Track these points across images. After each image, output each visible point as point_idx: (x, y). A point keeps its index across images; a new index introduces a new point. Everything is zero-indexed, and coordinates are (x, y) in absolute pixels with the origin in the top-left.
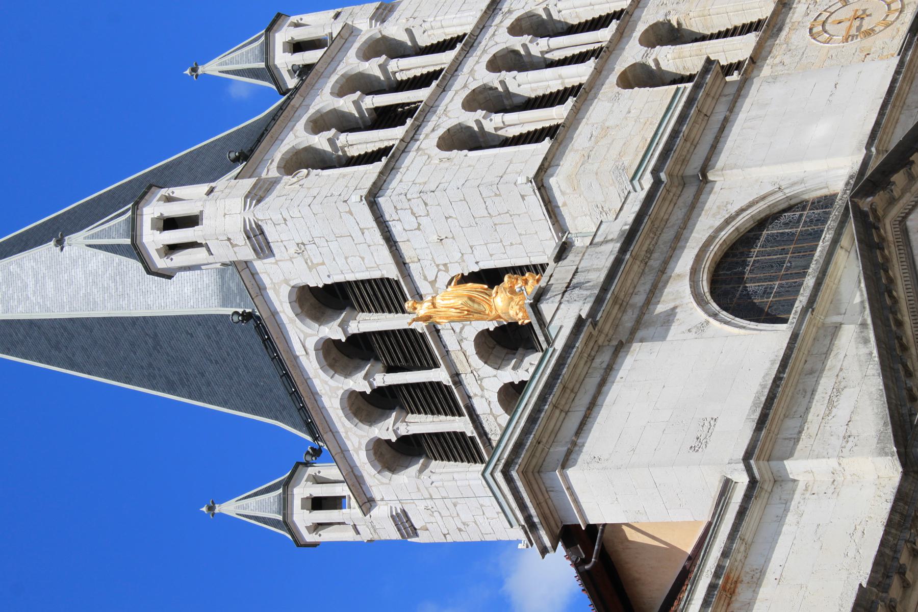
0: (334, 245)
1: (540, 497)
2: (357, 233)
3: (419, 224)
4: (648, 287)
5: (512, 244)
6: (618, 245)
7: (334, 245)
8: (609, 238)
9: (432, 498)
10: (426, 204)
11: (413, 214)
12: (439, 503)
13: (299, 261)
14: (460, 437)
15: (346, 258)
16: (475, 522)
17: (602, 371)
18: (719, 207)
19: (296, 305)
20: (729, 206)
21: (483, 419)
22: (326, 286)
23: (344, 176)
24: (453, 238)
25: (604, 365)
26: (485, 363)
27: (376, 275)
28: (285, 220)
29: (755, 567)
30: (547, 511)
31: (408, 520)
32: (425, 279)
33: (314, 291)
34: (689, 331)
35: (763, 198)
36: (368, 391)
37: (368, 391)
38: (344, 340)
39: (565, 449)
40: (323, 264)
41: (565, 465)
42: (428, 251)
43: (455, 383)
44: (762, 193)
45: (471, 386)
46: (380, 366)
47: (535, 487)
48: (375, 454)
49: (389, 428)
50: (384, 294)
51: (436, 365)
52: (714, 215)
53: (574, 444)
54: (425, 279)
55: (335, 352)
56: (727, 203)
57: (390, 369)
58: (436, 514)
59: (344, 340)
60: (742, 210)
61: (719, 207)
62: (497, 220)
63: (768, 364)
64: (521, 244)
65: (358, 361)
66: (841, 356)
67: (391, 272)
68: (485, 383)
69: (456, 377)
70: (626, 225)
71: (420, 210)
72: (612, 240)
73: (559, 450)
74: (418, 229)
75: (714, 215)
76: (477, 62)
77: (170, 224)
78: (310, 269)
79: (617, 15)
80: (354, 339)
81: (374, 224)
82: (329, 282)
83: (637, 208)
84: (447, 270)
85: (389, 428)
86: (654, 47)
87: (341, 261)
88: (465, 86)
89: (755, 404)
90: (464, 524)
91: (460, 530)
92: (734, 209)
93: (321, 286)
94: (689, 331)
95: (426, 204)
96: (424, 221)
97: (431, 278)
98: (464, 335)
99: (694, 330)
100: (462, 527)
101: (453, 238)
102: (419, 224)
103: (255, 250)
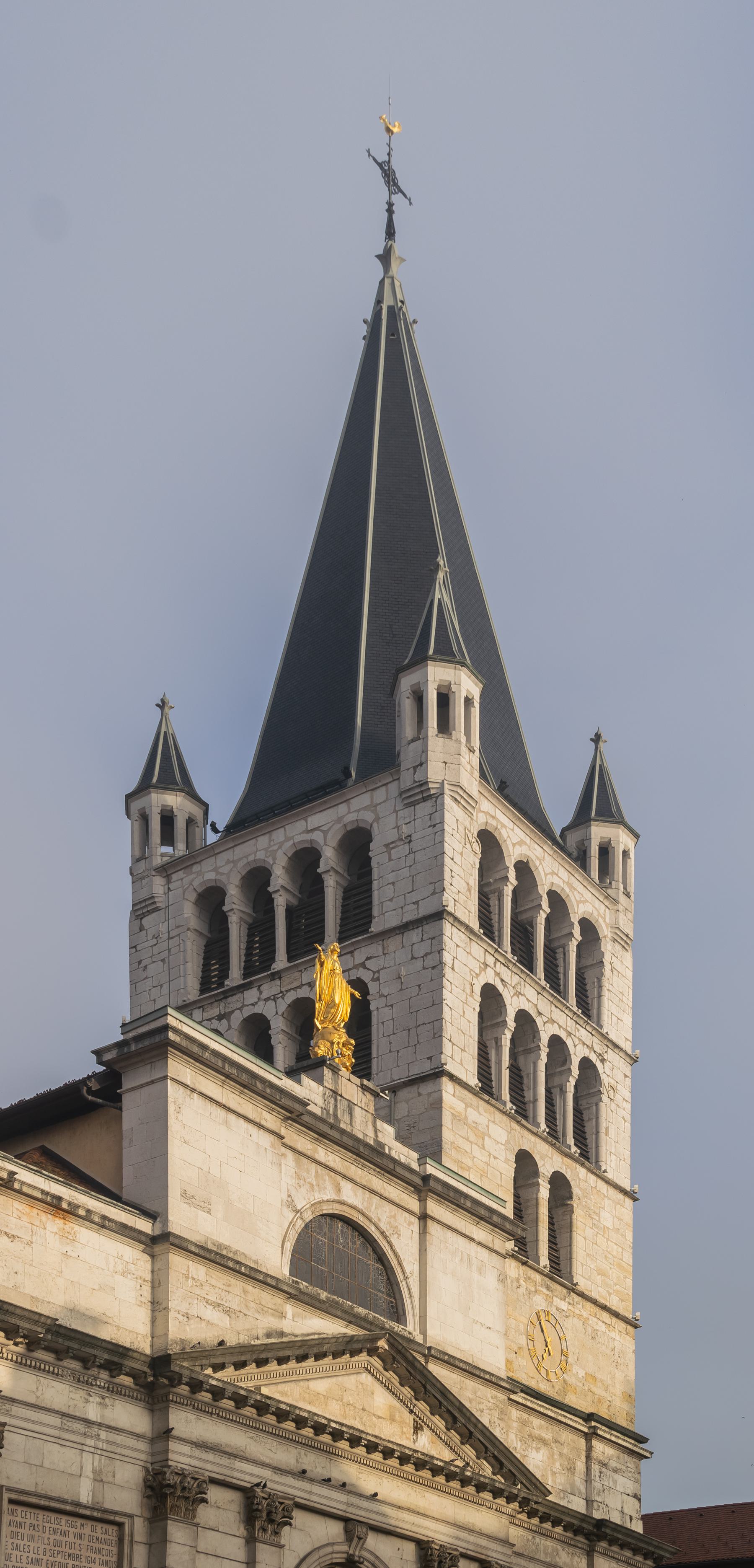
0: (405, 872)
2: (414, 897)
6: (372, 1142)
7: (405, 872)
8: (379, 1134)
9: (169, 938)
11: (427, 954)
14: (224, 973)
15: (393, 883)
16: (146, 978)
18: (396, 1227)
20: (396, 1236)
21: (239, 996)
23: (469, 890)
24: (401, 990)
26: (289, 1005)
27: (375, 912)
31: (150, 912)
32: (368, 959)
34: (289, 1196)
35: (400, 1264)
42: (392, 964)
43: (273, 974)
44: (405, 1264)
45: (270, 989)
46: (294, 902)
49: (236, 905)
50: (357, 921)
51: (290, 959)
52: (389, 1223)
54: (368, 959)
56: (399, 1235)
57: (290, 912)
58: (155, 941)
60: (391, 1246)
61: (396, 1227)
62: (413, 1031)
63: (254, 1258)
64: (390, 1051)
66: (257, 1316)
67: (375, 928)
68: (271, 1003)
69: (276, 976)
70: (390, 1149)
72: (377, 1136)
74: (413, 958)
75: (389, 1223)
78: (387, 846)
81: (420, 915)
82: (374, 864)
83: (403, 1160)
84: (373, 980)
85: (236, 905)
86: (550, 1183)
87: (391, 877)
89: (220, 1245)
90: (146, 967)
91: (140, 962)
92: (394, 1240)
94: (289, 1196)
96: (419, 964)
97: (369, 964)
99: (289, 1199)
100: (142, 965)
101: (401, 990)
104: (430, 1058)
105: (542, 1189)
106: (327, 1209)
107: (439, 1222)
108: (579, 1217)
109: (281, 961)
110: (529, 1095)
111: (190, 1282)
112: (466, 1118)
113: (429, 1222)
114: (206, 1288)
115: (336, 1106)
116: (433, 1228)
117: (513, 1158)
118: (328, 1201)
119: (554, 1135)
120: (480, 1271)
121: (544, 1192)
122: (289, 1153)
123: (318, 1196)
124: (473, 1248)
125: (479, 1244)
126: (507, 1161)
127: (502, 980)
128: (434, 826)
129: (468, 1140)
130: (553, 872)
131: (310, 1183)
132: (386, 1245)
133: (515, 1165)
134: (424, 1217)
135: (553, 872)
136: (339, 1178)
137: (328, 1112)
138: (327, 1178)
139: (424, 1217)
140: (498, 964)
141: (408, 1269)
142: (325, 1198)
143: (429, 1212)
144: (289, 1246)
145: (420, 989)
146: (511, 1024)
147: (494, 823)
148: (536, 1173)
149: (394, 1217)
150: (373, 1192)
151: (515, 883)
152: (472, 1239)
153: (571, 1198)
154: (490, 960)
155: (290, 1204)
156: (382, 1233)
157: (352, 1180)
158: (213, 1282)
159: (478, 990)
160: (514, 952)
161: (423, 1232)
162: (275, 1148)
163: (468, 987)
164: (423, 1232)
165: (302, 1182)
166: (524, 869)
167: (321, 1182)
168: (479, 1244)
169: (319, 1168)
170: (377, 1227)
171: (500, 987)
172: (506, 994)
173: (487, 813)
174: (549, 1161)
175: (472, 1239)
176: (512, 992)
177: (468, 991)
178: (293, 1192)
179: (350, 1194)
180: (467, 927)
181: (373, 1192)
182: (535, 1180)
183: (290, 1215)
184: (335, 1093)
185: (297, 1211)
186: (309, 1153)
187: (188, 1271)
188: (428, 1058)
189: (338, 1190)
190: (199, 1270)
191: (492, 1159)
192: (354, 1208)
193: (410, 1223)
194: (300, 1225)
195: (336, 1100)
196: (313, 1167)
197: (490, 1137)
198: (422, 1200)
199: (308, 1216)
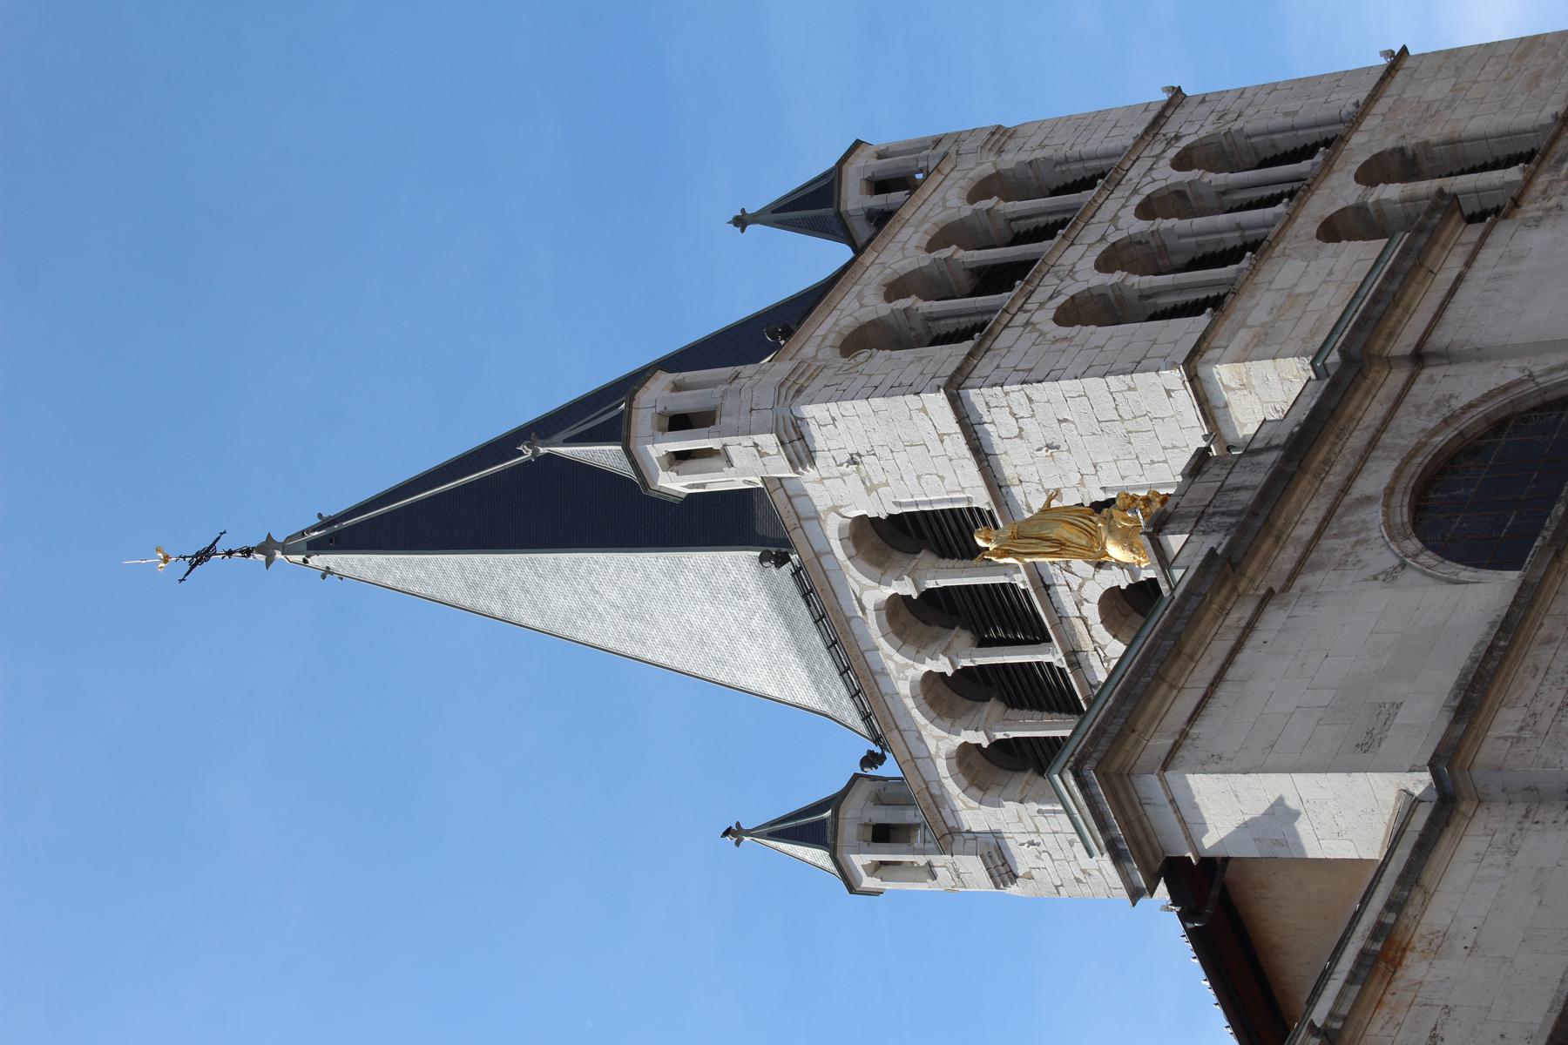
1: (1130, 812)
3: (1021, 429)
4: (1321, 514)
5: (1153, 462)
8: (1274, 443)
9: (1038, 832)
10: (1030, 400)
12: (1049, 839)
13: (853, 480)
15: (919, 477)
16: (1099, 870)
17: (1238, 632)
19: (850, 543)
20: (1453, 401)
22: (891, 517)
23: (921, 358)
25: (1243, 623)
26: (1115, 636)
28: (834, 419)
29: (1436, 928)
30: (1140, 835)
33: (875, 521)
36: (950, 672)
37: (950, 672)
38: (915, 596)
39: (1171, 742)
40: (887, 484)
41: (1166, 765)
42: (1032, 469)
43: (1070, 664)
47: (1123, 796)
48: (960, 764)
52: (1429, 414)
53: (1184, 734)
55: (905, 614)
56: (1451, 396)
57: (984, 643)
58: (1045, 856)
59: (915, 596)
60: (1471, 406)
61: (1437, 402)
62: (1129, 425)
65: (937, 629)
71: (1023, 411)
73: (1160, 743)
75: (1429, 414)
76: (1124, 206)
77: (679, 422)
79: (1327, 143)
80: (928, 595)
81: (957, 428)
87: (910, 479)
88: (1103, 238)
89: (1458, 685)
90: (1084, 871)
91: (1078, 880)
92: (1457, 404)
93: (883, 517)
94: (1375, 578)
95: (1030, 400)
98: (1085, 593)
100: (1082, 877)
102: (1021, 429)
103: (790, 462)
104: (1168, 392)
105: (1384, 196)
106: (1402, 514)
107: (1428, 333)
108: (1433, 132)
109: (1053, 656)
110: (1232, 240)
111: (1526, 734)
112: (1263, 325)
113: (1428, 347)
114: (1539, 707)
115: (1223, 513)
116: (1441, 338)
117: (1332, 247)
118: (1385, 514)
119: (1296, 193)
120: (1519, 258)
121: (1391, 192)
122: (1300, 582)
123: (1377, 529)
124: (1478, 274)
125: (1468, 265)
126: (1336, 255)
127: (1051, 298)
128: (834, 419)
129: (1299, 319)
130: (904, 249)
131: (1354, 547)
132: (1468, 415)
133: (1344, 242)
134: (1419, 357)
135: (904, 249)
136: (1347, 500)
137: (1232, 525)
138: (1346, 519)
139: (1419, 357)
140: (1027, 307)
141: (1514, 375)
142: (1381, 518)
143: (1409, 350)
144: (1466, 573)
145: (1065, 420)
146: (1117, 276)
147: (832, 336)
148: (1360, 209)
149: (1418, 407)
150: (1372, 444)
151: (913, 298)
152: (1460, 278)
153: (1402, 150)
154: (1021, 318)
155: (1390, 576)
156: (1446, 422)
157: (1351, 480)
158: (1529, 694)
159: (1064, 331)
160: (1010, 288)
161: (1447, 356)
162: (1289, 603)
163: (1059, 346)
164: (1447, 356)
165: (1351, 559)
166: (895, 290)
167: (1353, 528)
168: (1468, 265)
169: (1328, 532)
170: (1435, 432)
171: (1061, 300)
172: (1072, 289)
173: (819, 347)
174: (1340, 191)
175: (1460, 278)
176: (1068, 281)
177: (1065, 344)
178: (1370, 572)
179: (1375, 480)
180: (971, 355)
181: (1372, 444)
182: (1371, 209)
183: (1409, 576)
184: (1201, 516)
185: (1404, 565)
186: (1300, 551)
187: (1505, 738)
188: (1170, 396)
189: (1368, 500)
190: (1506, 720)
191: (1333, 278)
192: (1398, 473)
193: (1431, 380)
194: (1428, 558)
195: (1214, 514)
196: (1325, 543)
197: (1295, 285)
198: (1389, 362)
199: (1413, 545)
